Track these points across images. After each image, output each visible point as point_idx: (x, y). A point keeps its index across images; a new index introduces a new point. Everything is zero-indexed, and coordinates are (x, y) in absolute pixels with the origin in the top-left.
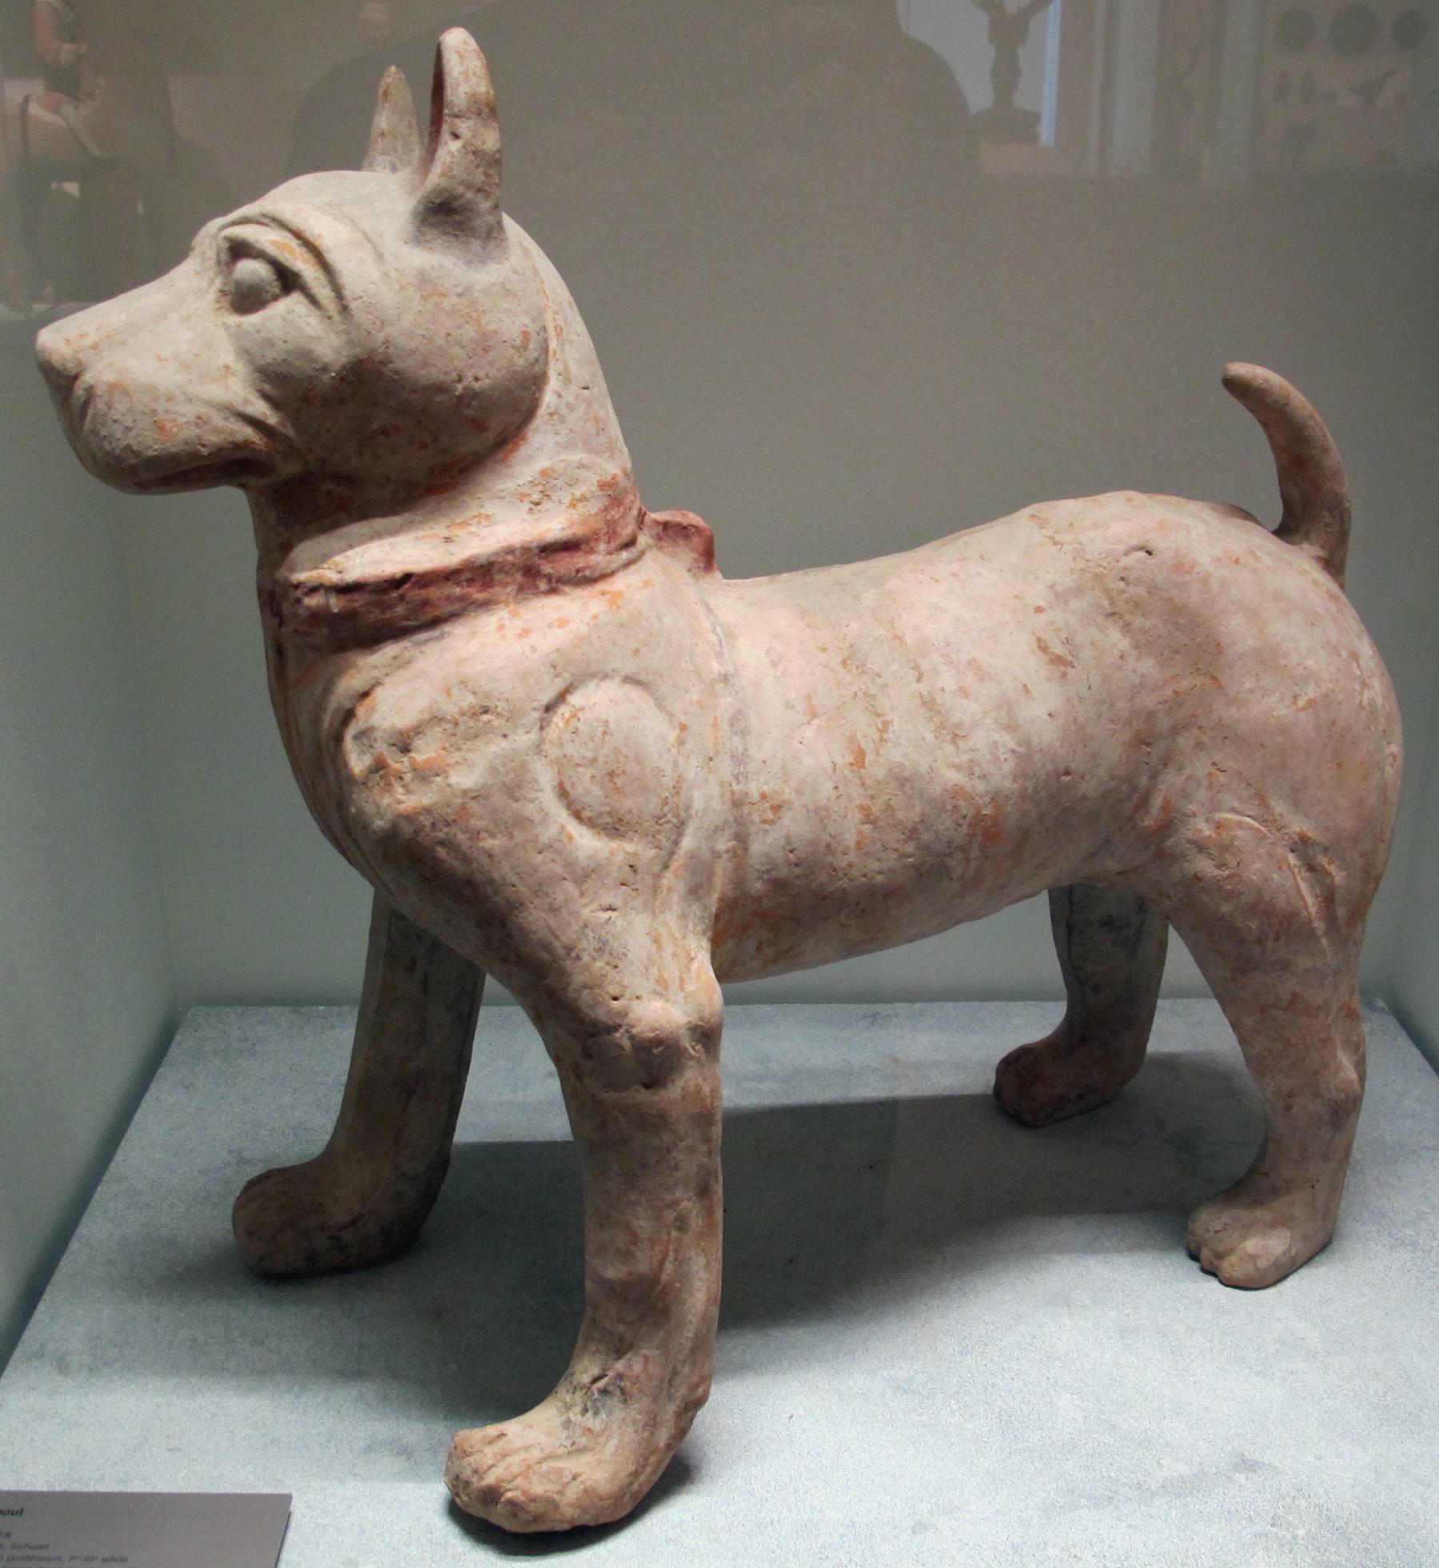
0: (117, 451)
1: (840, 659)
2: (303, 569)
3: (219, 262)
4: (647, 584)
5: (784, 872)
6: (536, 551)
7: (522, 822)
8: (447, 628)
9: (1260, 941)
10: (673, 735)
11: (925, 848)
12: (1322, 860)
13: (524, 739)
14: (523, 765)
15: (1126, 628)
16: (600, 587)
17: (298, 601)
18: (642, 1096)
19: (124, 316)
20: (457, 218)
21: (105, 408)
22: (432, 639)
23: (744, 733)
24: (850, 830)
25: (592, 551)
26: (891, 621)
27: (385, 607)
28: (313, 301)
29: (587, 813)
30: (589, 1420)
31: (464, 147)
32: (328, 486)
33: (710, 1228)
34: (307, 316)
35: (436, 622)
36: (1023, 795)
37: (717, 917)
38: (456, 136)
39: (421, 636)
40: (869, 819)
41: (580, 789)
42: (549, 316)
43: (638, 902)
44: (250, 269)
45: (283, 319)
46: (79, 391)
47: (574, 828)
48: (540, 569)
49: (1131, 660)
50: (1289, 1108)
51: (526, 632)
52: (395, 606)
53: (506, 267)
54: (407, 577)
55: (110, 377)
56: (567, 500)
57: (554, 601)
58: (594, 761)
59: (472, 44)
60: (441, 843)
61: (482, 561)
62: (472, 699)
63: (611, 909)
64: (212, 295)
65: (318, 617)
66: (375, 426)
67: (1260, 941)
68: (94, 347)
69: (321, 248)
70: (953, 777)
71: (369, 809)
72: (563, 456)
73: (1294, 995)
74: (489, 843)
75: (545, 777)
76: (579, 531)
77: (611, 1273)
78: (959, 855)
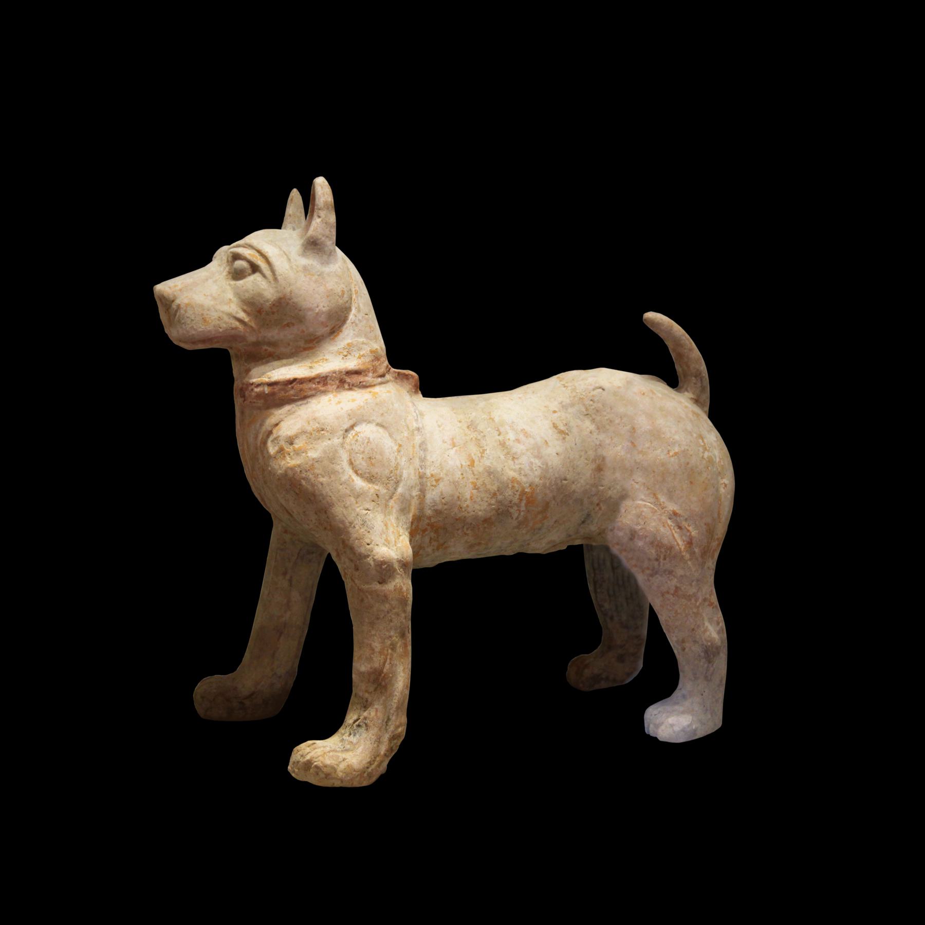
1: (466, 425)
4: (389, 392)
5: (440, 507)
7: (335, 472)
9: (657, 560)
10: (395, 448)
11: (500, 502)
12: (685, 524)
13: (336, 441)
14: (336, 451)
15: (593, 420)
16: (369, 389)
18: (377, 586)
19: (191, 280)
23: (425, 450)
24: (468, 492)
25: (366, 375)
26: (490, 413)
27: (286, 391)
28: (264, 276)
29: (360, 472)
30: (352, 738)
33: (406, 652)
35: (305, 398)
36: (544, 485)
37: (412, 523)
38: (319, 217)
40: (475, 487)
41: (358, 462)
42: (353, 286)
43: (379, 509)
44: (240, 264)
46: (174, 306)
47: (354, 477)
48: (346, 380)
49: (595, 434)
50: (684, 649)
51: (339, 402)
53: (337, 266)
54: (295, 380)
55: (186, 301)
56: (357, 355)
57: (350, 393)
58: (363, 452)
59: (326, 183)
60: (304, 479)
62: (317, 425)
63: (368, 509)
64: (225, 273)
65: (260, 396)
67: (657, 560)
68: (181, 290)
70: (512, 474)
71: (276, 467)
73: (677, 588)
74: (321, 479)
75: (345, 456)
76: (362, 367)
77: (363, 668)
78: (515, 508)
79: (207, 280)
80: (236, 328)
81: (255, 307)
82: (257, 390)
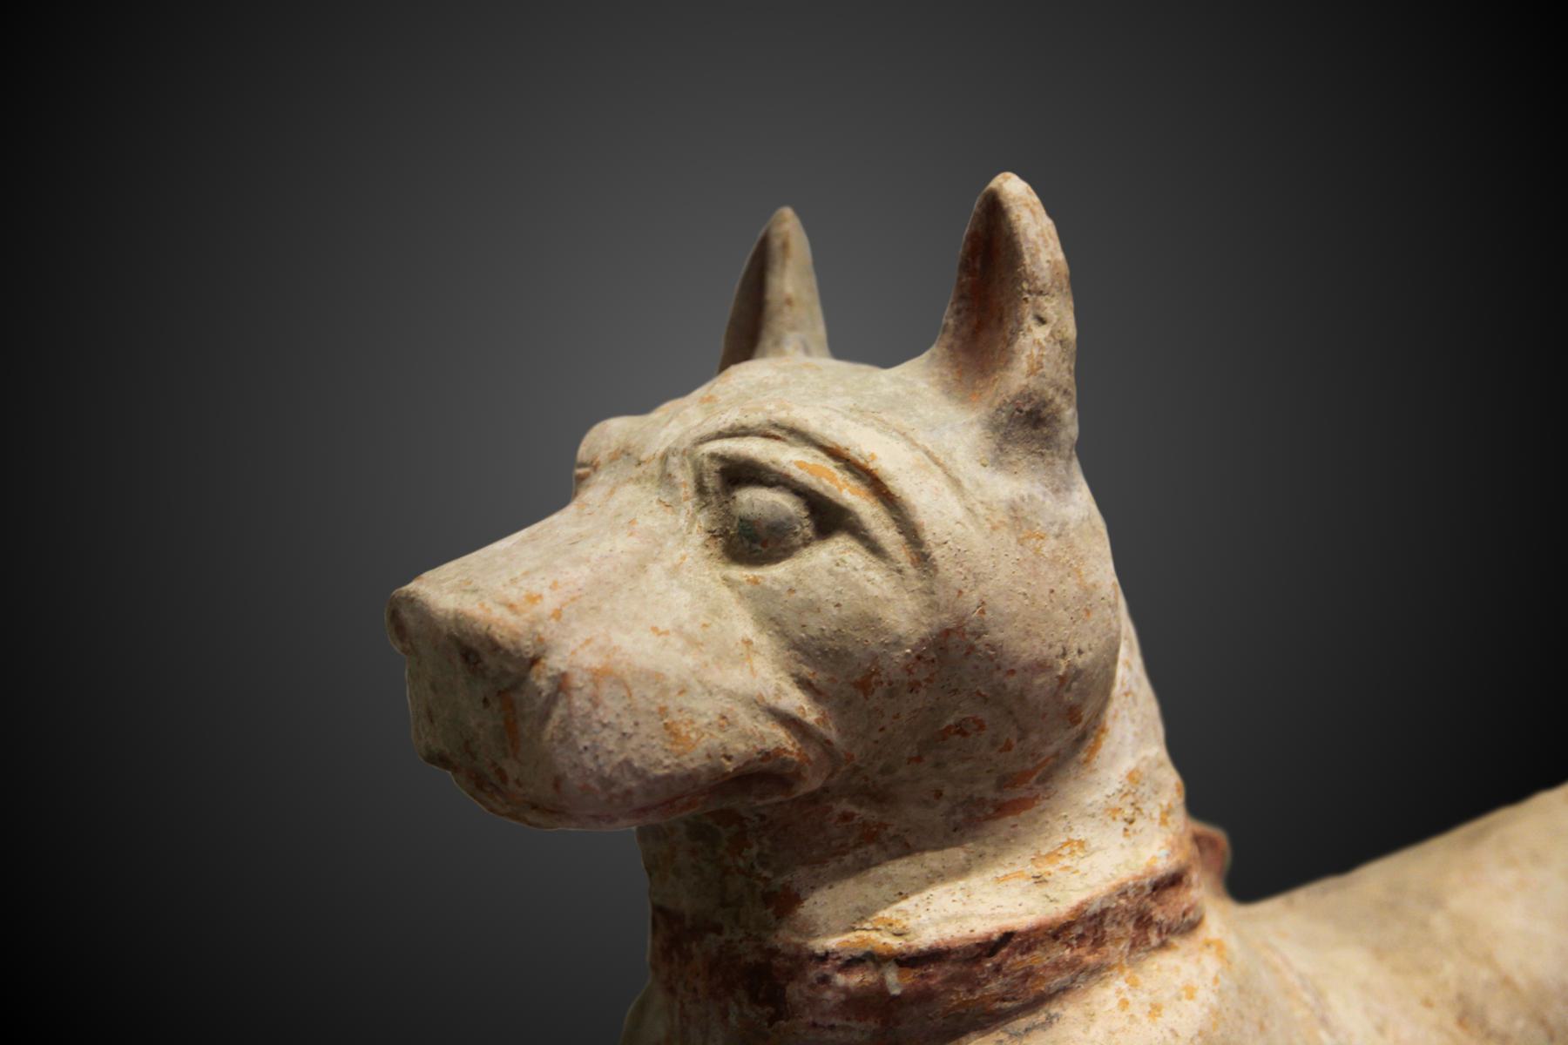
0: (608, 770)
2: (831, 932)
3: (701, 489)
6: (1148, 890)
8: (1054, 1009)
17: (825, 980)
20: (1045, 431)
21: (588, 705)
22: (1035, 1027)
27: (973, 983)
31: (1052, 334)
32: (844, 806)
34: (867, 568)
35: (1041, 1000)
38: (1042, 321)
39: (1023, 1023)
44: (756, 500)
45: (830, 572)
51: (1156, 1009)
52: (988, 981)
54: (1008, 936)
55: (591, 660)
56: (1156, 814)
57: (1166, 960)
61: (1095, 908)
64: (697, 538)
66: (951, 721)
68: (557, 614)
69: (880, 474)
72: (1143, 753)
79: (643, 567)
80: (779, 751)
81: (834, 662)
82: (854, 979)
